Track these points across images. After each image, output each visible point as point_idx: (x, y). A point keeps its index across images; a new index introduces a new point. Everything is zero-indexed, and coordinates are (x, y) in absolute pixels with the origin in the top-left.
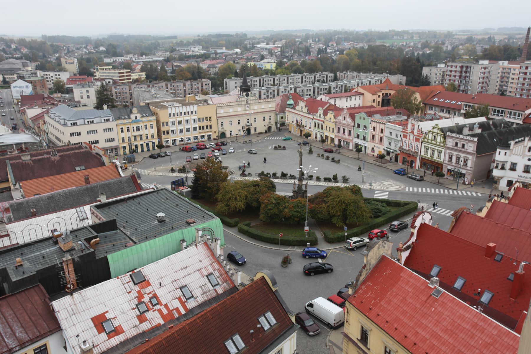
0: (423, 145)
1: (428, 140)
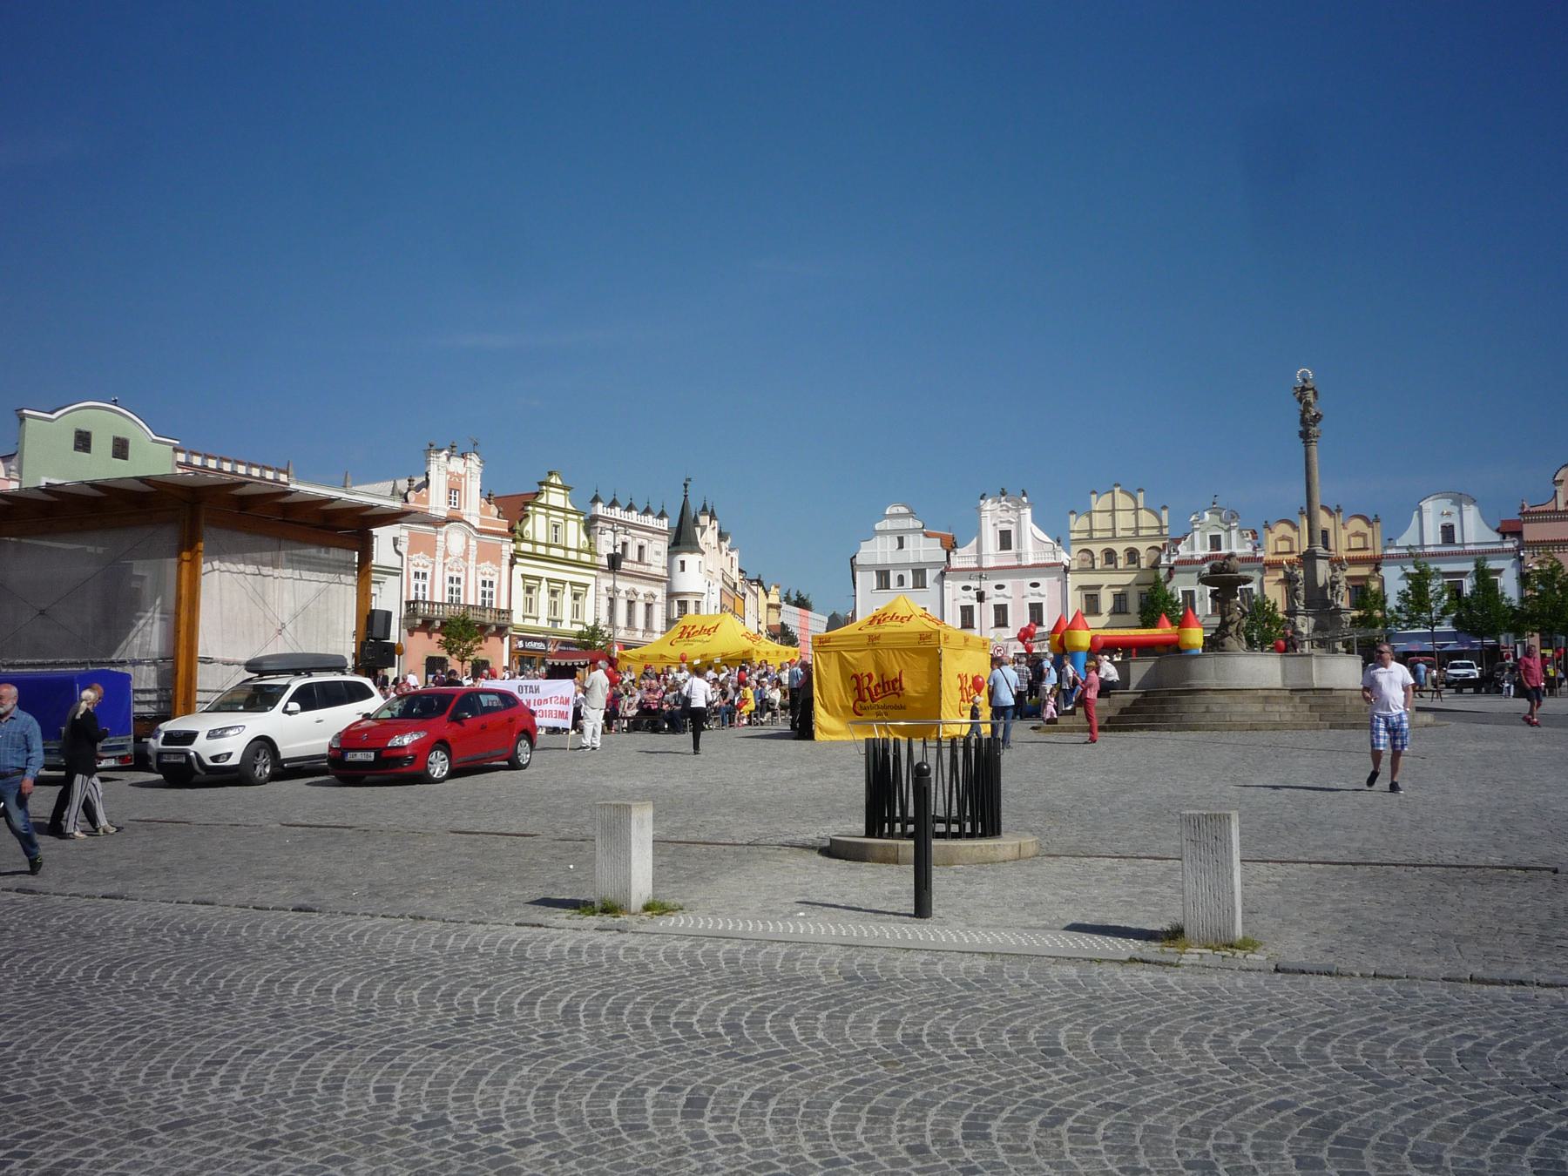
0: (518, 570)
1: (534, 543)
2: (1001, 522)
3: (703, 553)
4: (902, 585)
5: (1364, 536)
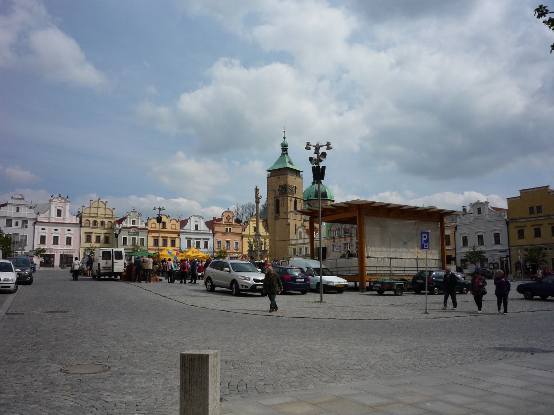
2: (58, 206)
5: (175, 225)
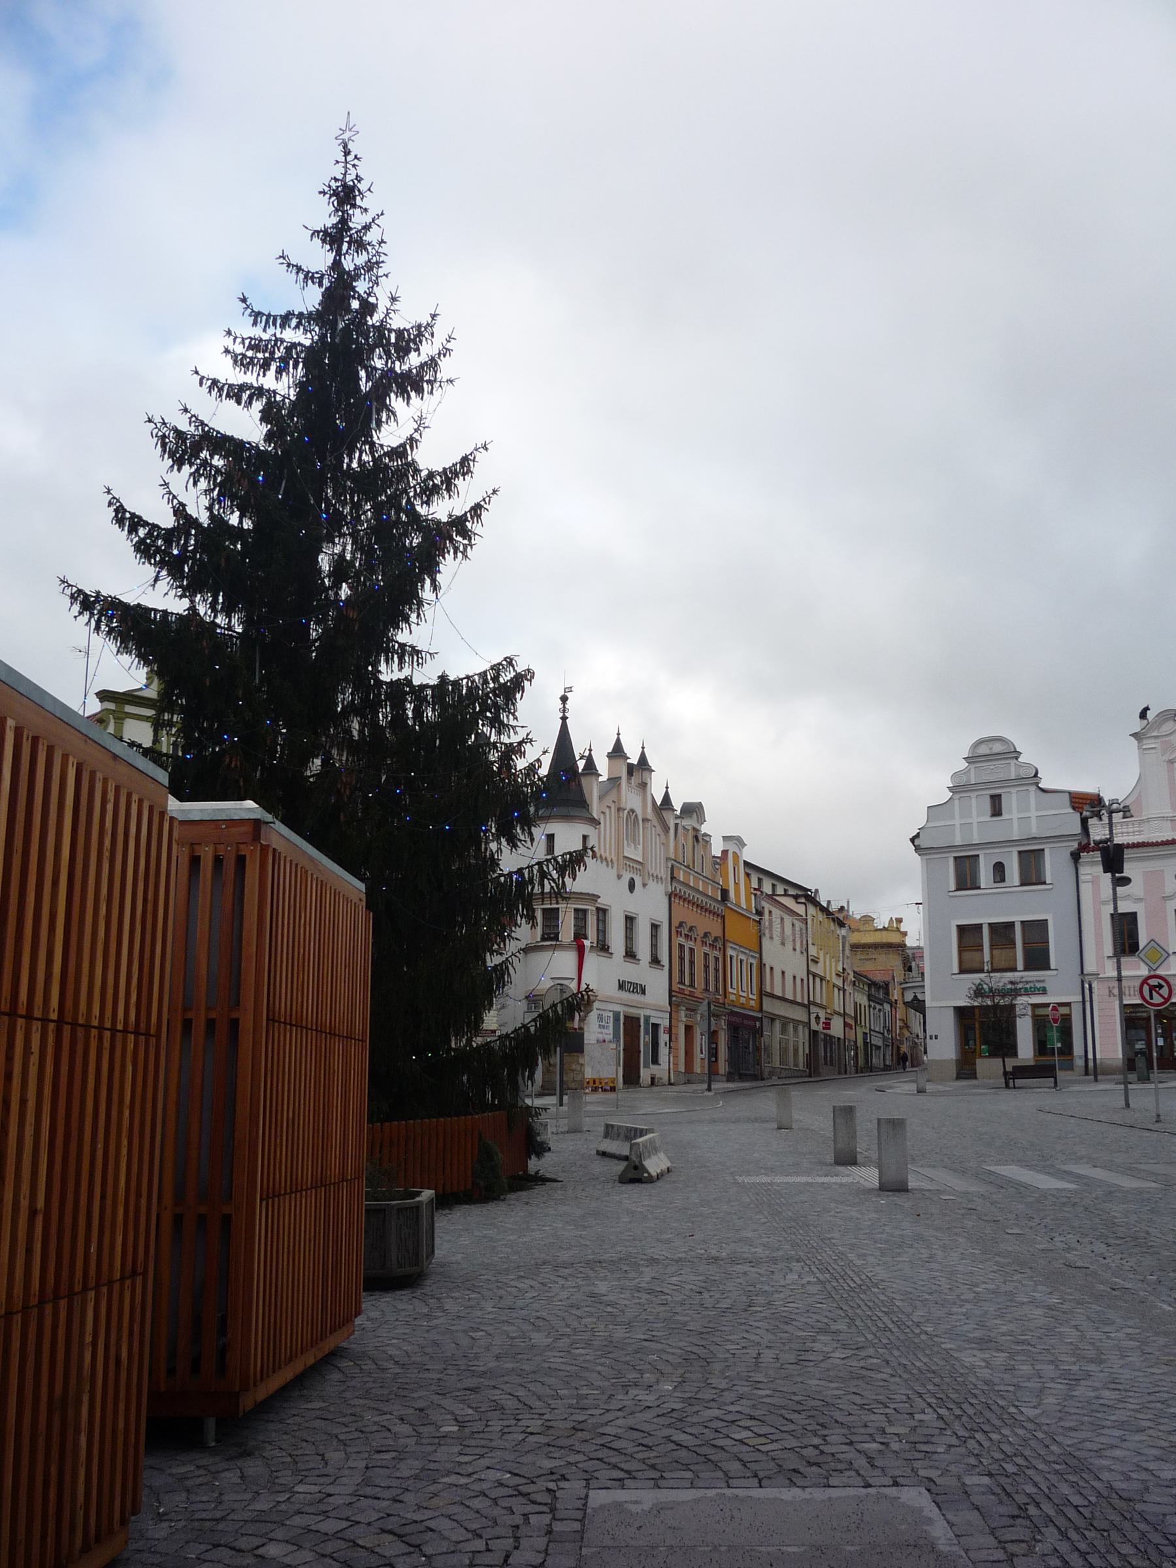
3: (595, 822)
4: (1003, 880)
